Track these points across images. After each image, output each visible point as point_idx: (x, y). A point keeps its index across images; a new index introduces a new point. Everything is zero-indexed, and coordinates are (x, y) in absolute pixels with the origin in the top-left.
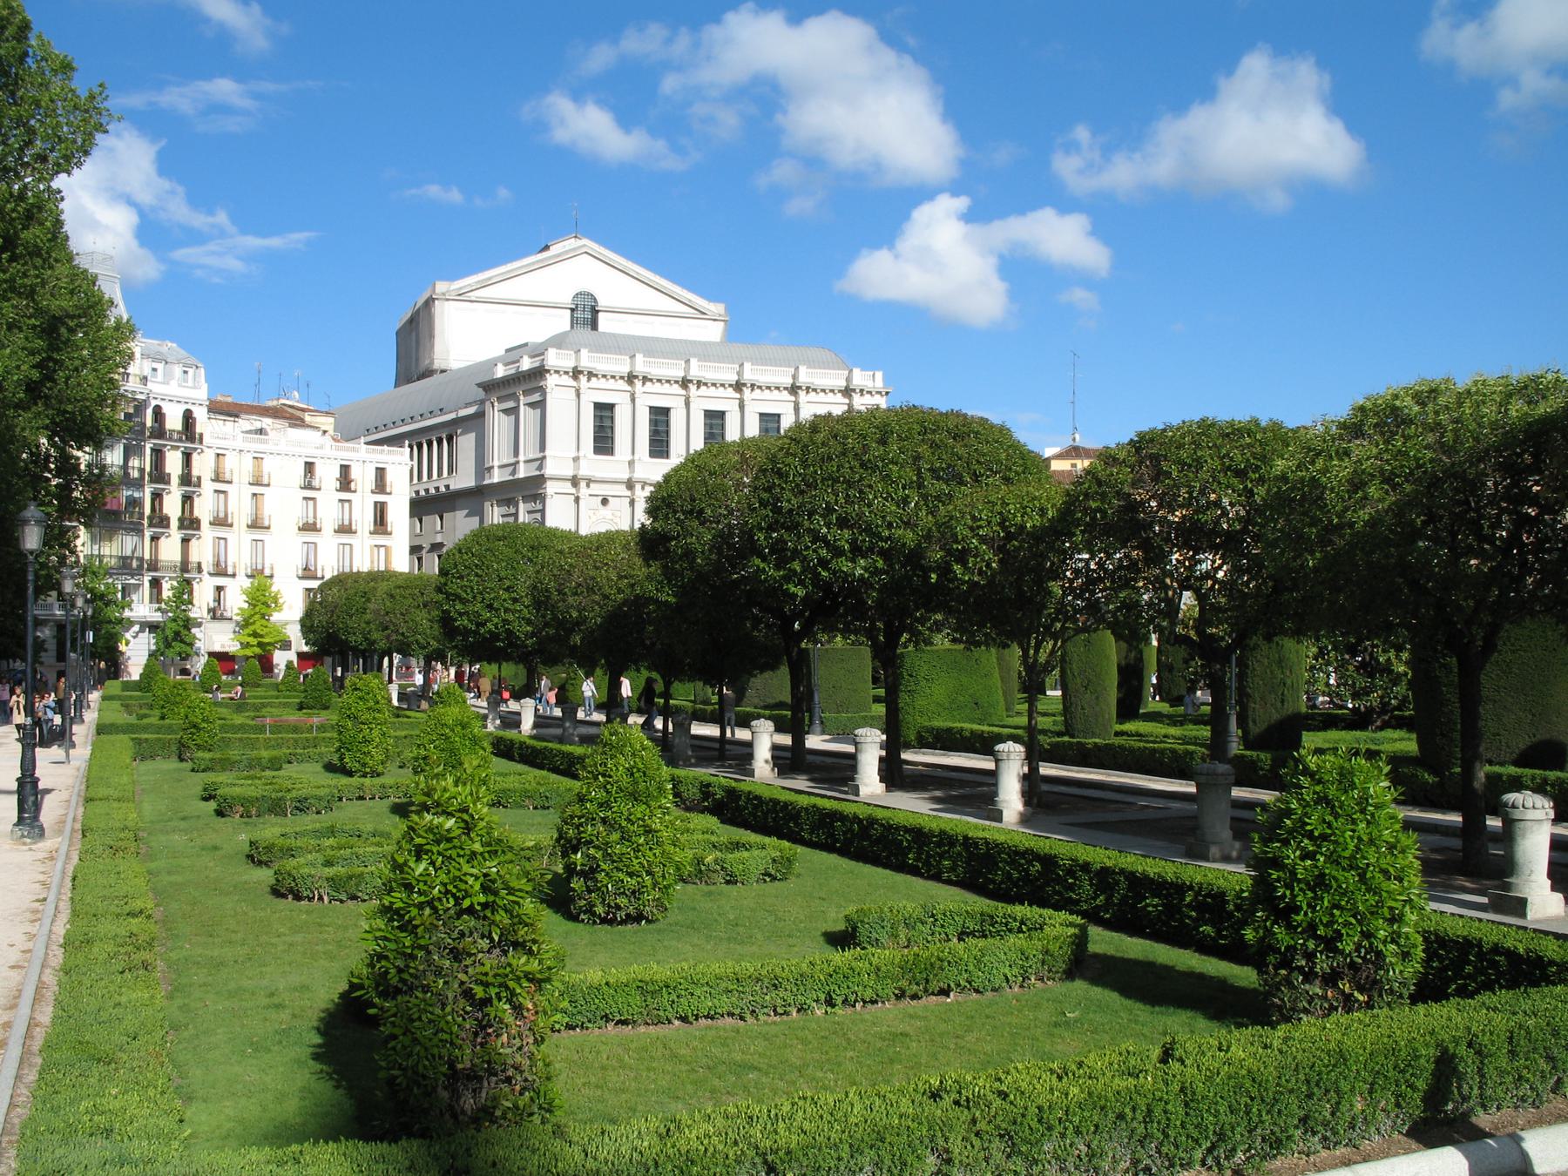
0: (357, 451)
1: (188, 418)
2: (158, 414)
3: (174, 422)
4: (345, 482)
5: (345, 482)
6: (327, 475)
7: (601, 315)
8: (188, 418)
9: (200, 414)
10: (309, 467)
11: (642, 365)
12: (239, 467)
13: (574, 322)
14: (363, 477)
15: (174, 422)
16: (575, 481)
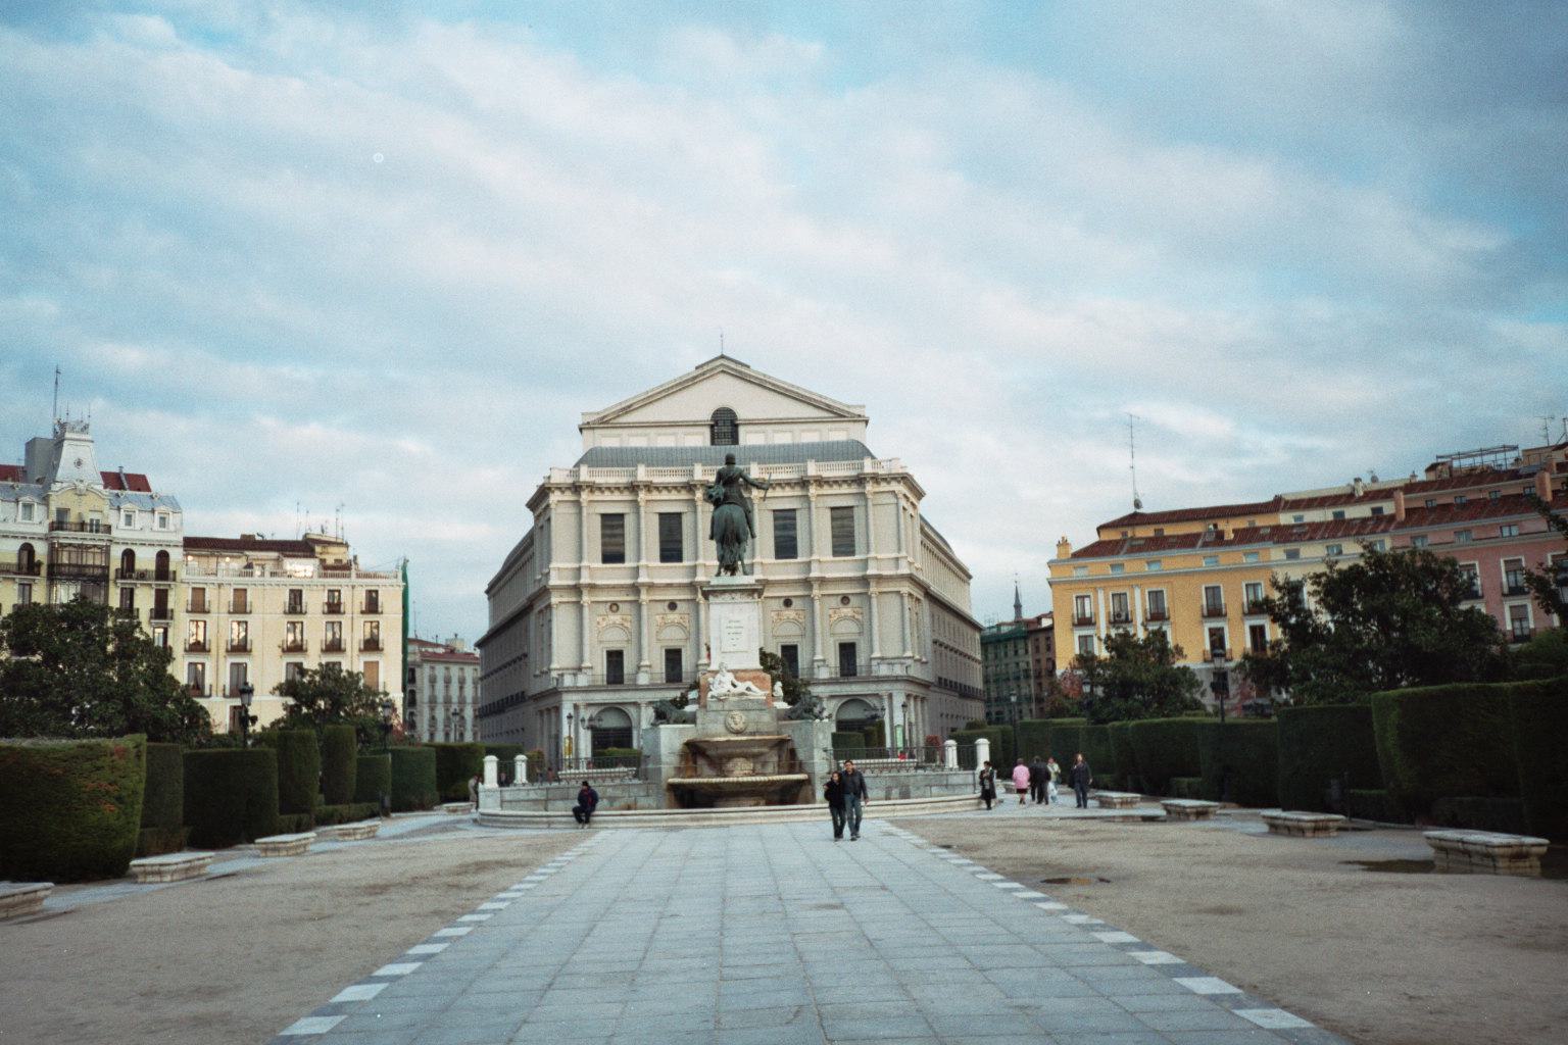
0: (349, 576)
1: (163, 557)
2: (129, 556)
3: (146, 560)
4: (334, 608)
5: (334, 608)
6: (314, 601)
7: (742, 430)
8: (163, 557)
9: (176, 555)
10: (296, 596)
11: (642, 474)
12: (219, 599)
13: (715, 439)
14: (353, 598)
15: (146, 560)
16: (577, 589)
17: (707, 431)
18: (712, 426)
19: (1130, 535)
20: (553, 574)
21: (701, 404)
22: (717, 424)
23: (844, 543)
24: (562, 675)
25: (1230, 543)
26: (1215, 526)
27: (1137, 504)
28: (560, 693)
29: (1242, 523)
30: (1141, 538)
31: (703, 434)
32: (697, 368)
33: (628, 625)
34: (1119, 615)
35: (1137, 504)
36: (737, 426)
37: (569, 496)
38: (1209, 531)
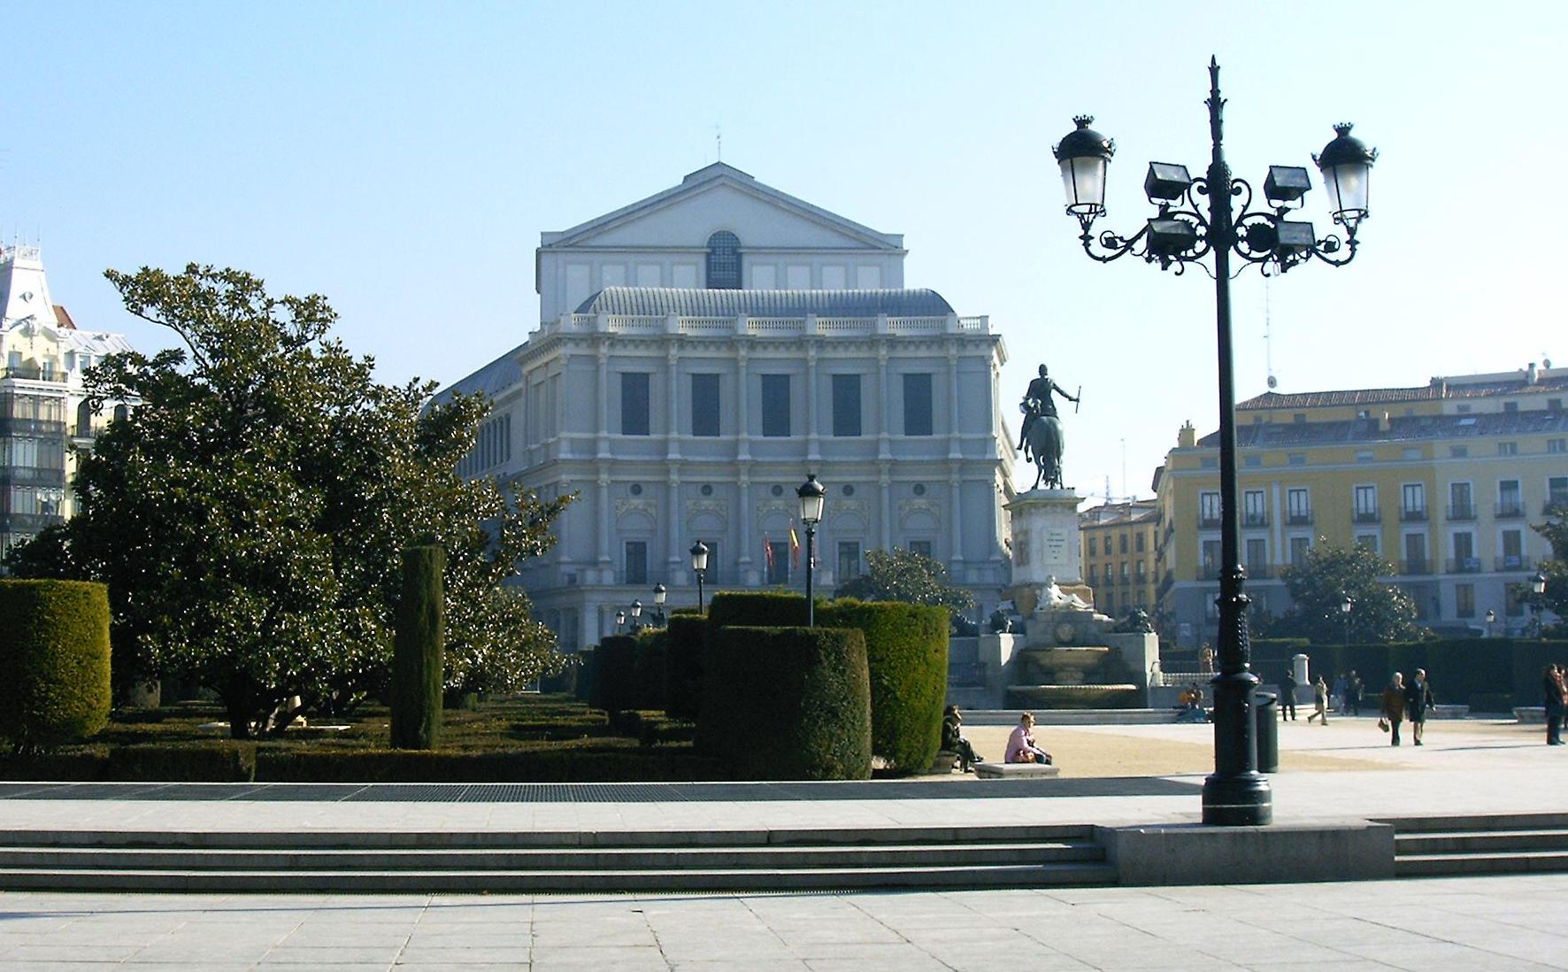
7: (746, 261)
17: (702, 261)
18: (708, 255)
19: (1265, 419)
20: (564, 446)
21: (695, 225)
22: (714, 252)
23: (918, 417)
24: (583, 571)
25: (1384, 435)
26: (1367, 413)
27: (1272, 382)
28: (582, 592)
29: (1401, 411)
30: (1278, 426)
31: (696, 264)
32: (686, 178)
33: (652, 511)
34: (1253, 517)
35: (1272, 382)
36: (740, 255)
37: (583, 350)
38: (1360, 420)
